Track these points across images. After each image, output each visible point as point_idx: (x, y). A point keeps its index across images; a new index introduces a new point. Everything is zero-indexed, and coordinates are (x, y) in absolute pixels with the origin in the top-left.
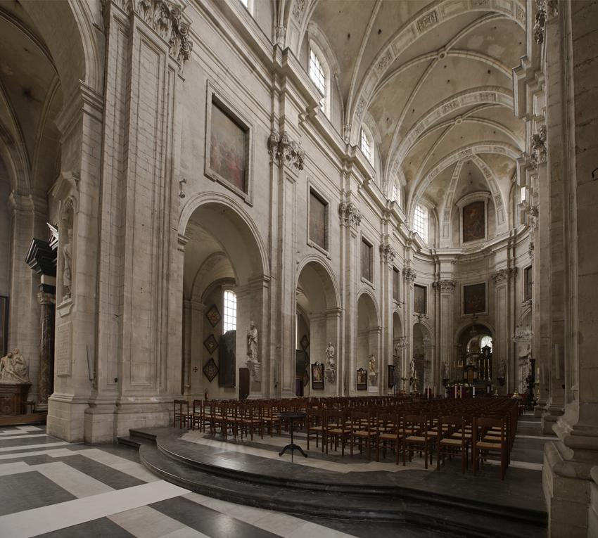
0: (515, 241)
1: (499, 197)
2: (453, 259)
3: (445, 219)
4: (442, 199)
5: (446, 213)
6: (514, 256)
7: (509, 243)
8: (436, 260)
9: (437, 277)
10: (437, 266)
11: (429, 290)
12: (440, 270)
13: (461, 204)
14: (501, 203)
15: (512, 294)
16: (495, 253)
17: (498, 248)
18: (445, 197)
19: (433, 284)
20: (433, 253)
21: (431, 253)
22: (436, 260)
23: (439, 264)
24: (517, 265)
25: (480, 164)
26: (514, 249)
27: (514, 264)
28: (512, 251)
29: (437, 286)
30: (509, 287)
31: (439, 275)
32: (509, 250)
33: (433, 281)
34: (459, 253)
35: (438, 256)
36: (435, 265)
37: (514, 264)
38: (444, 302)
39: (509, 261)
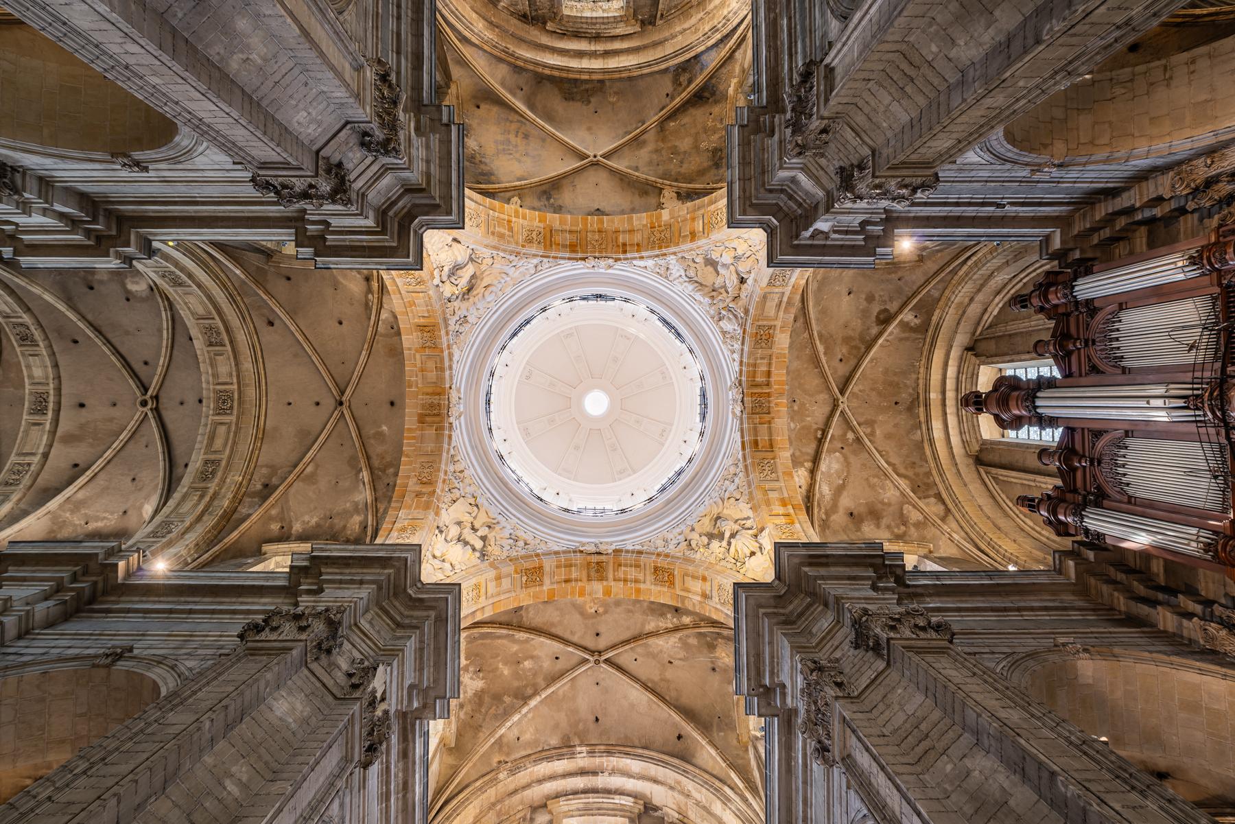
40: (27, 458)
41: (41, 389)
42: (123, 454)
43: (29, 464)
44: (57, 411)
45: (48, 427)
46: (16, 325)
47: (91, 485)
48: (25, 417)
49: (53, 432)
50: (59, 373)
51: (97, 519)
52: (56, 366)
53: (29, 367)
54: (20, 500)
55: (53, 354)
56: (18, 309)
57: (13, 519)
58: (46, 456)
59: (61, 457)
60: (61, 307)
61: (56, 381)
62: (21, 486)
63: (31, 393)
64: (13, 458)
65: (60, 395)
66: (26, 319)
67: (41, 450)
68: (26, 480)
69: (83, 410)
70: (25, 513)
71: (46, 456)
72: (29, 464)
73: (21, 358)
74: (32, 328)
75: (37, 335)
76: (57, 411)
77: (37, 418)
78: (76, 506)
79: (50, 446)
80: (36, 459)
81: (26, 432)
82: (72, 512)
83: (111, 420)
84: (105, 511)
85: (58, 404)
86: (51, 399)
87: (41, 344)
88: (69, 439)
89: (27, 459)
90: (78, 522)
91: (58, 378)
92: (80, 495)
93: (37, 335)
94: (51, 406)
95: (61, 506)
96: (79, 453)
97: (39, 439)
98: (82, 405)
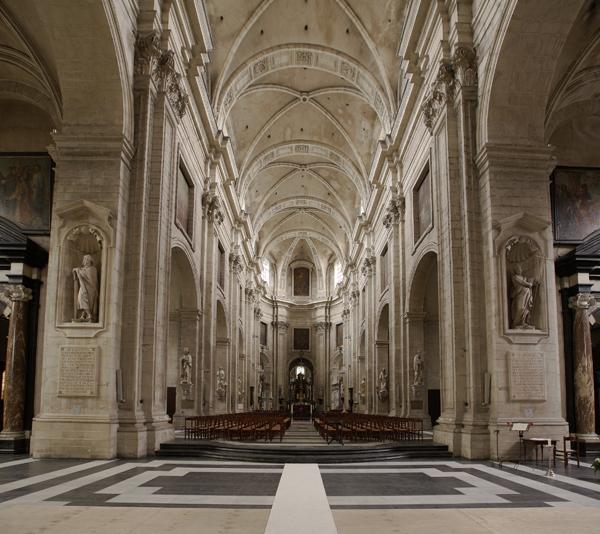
1: (320, 271)
3: (283, 275)
4: (281, 259)
5: (283, 270)
11: (269, 326)
13: (293, 266)
14: (321, 275)
18: (283, 258)
19: (272, 323)
25: (310, 244)
29: (275, 325)
35: (277, 302)
38: (280, 338)
41: (295, 57)
44: (309, 45)
45: (320, 52)
46: (255, 72)
47: (363, 18)
48: (313, 67)
49: (324, 48)
51: (389, 12)
52: (280, 46)
53: (281, 65)
55: (272, 49)
56: (245, 70)
60: (239, 40)
63: (298, 64)
64: (338, 74)
66: (251, 64)
68: (353, 65)
71: (338, 53)
73: (276, 69)
74: (257, 61)
75: (261, 58)
76: (309, 45)
77: (313, 60)
78: (377, 28)
79: (332, 49)
80: (340, 58)
81: (322, 66)
82: (379, 32)
84: (385, 6)
86: (302, 49)
87: (265, 56)
88: (329, 36)
89: (339, 64)
90: (387, 28)
91: (287, 45)
92: (369, 26)
93: (261, 58)
94: (306, 50)
95: (373, 40)
96: (339, 30)
97: (327, 59)
98: (306, 28)
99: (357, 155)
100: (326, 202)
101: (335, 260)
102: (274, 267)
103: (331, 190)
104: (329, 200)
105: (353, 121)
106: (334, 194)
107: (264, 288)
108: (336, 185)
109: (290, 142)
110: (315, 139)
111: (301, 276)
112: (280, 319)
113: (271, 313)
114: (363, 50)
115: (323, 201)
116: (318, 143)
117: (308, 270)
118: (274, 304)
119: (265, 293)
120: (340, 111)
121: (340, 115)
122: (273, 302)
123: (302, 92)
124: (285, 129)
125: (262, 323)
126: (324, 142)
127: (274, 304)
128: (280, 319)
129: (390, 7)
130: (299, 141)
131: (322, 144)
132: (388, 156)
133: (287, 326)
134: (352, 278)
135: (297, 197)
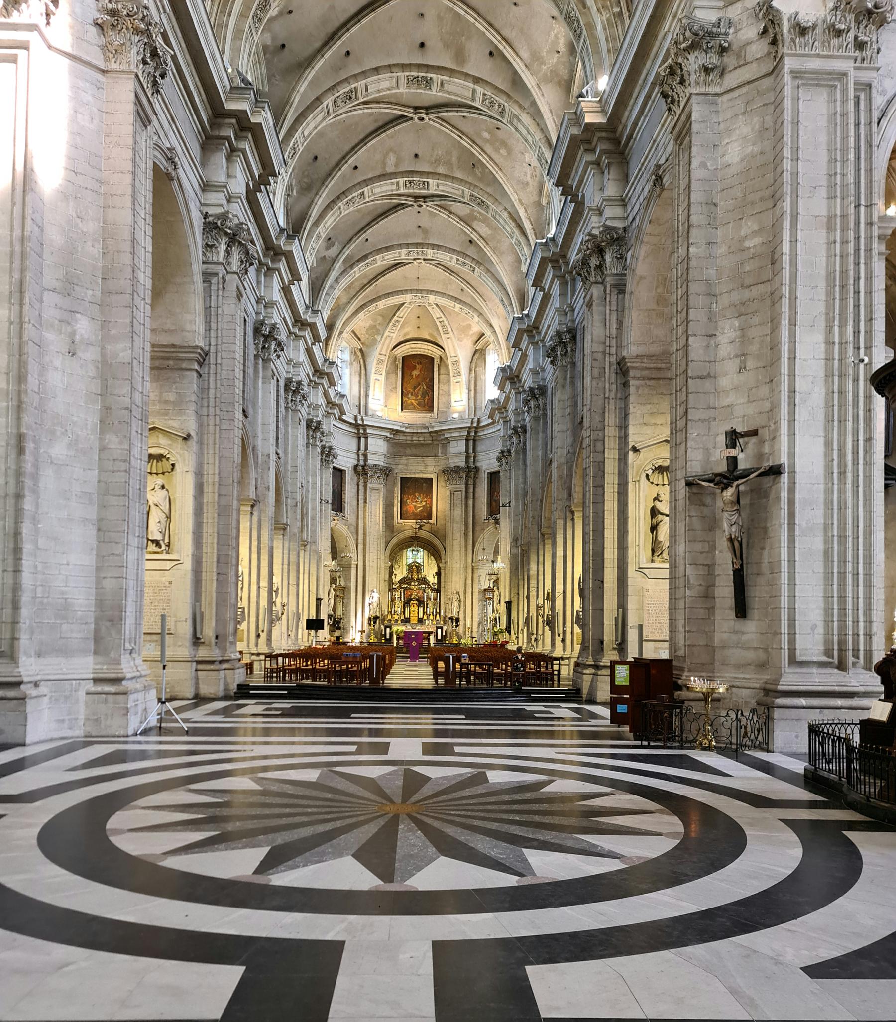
0: (476, 432)
1: (456, 363)
2: (388, 434)
6: (474, 451)
7: (469, 432)
8: (361, 431)
9: (361, 458)
10: (363, 440)
11: (349, 477)
12: (366, 448)
15: (471, 502)
16: (448, 440)
17: (453, 435)
19: (356, 467)
20: (359, 422)
21: (356, 419)
22: (361, 431)
23: (366, 438)
24: (478, 465)
26: (474, 441)
27: (474, 462)
28: (471, 443)
29: (362, 471)
30: (467, 492)
31: (365, 455)
32: (467, 440)
33: (356, 463)
34: (398, 428)
35: (365, 426)
36: (359, 438)
37: (474, 462)
39: (468, 457)
40: (478, 95)
42: (482, 10)
43: (485, 94)
48: (434, 92)
49: (451, 72)
50: (385, 66)
54: (520, 106)
57: (536, 114)
58: (477, 80)
59: (479, 65)
61: (394, 69)
62: (506, 104)
63: (408, 87)
65: (410, 65)
67: (471, 85)
69: (427, 44)
70: (534, 103)
71: (477, 80)
72: (485, 94)
76: (428, 68)
79: (467, 75)
80: (480, 90)
83: (440, 18)
85: (419, 67)
88: (460, 55)
98: (422, 45)
99: (516, 204)
100: (465, 255)
101: (487, 344)
102: (362, 356)
103: (474, 237)
104: (471, 252)
105: (509, 152)
106: (481, 244)
107: (340, 407)
108: (484, 230)
109: (394, 175)
110: (441, 170)
111: (415, 373)
112: (372, 460)
113: (354, 447)
114: (516, 81)
115: (458, 253)
116: (446, 177)
117: (433, 359)
118: (360, 431)
119: (343, 412)
120: (486, 135)
121: (487, 141)
122: (356, 426)
123: (416, 108)
124: (385, 156)
125: (334, 468)
126: (459, 174)
127: (360, 431)
128: (372, 460)
129: (556, 36)
130: (412, 173)
131: (454, 179)
132: (551, 261)
133: (386, 473)
134: (531, 358)
135: (408, 245)
